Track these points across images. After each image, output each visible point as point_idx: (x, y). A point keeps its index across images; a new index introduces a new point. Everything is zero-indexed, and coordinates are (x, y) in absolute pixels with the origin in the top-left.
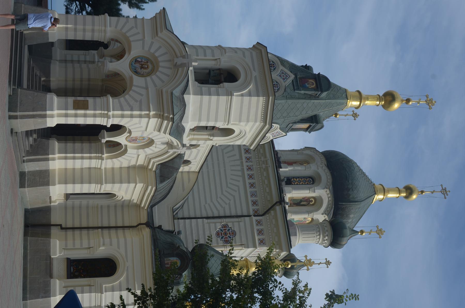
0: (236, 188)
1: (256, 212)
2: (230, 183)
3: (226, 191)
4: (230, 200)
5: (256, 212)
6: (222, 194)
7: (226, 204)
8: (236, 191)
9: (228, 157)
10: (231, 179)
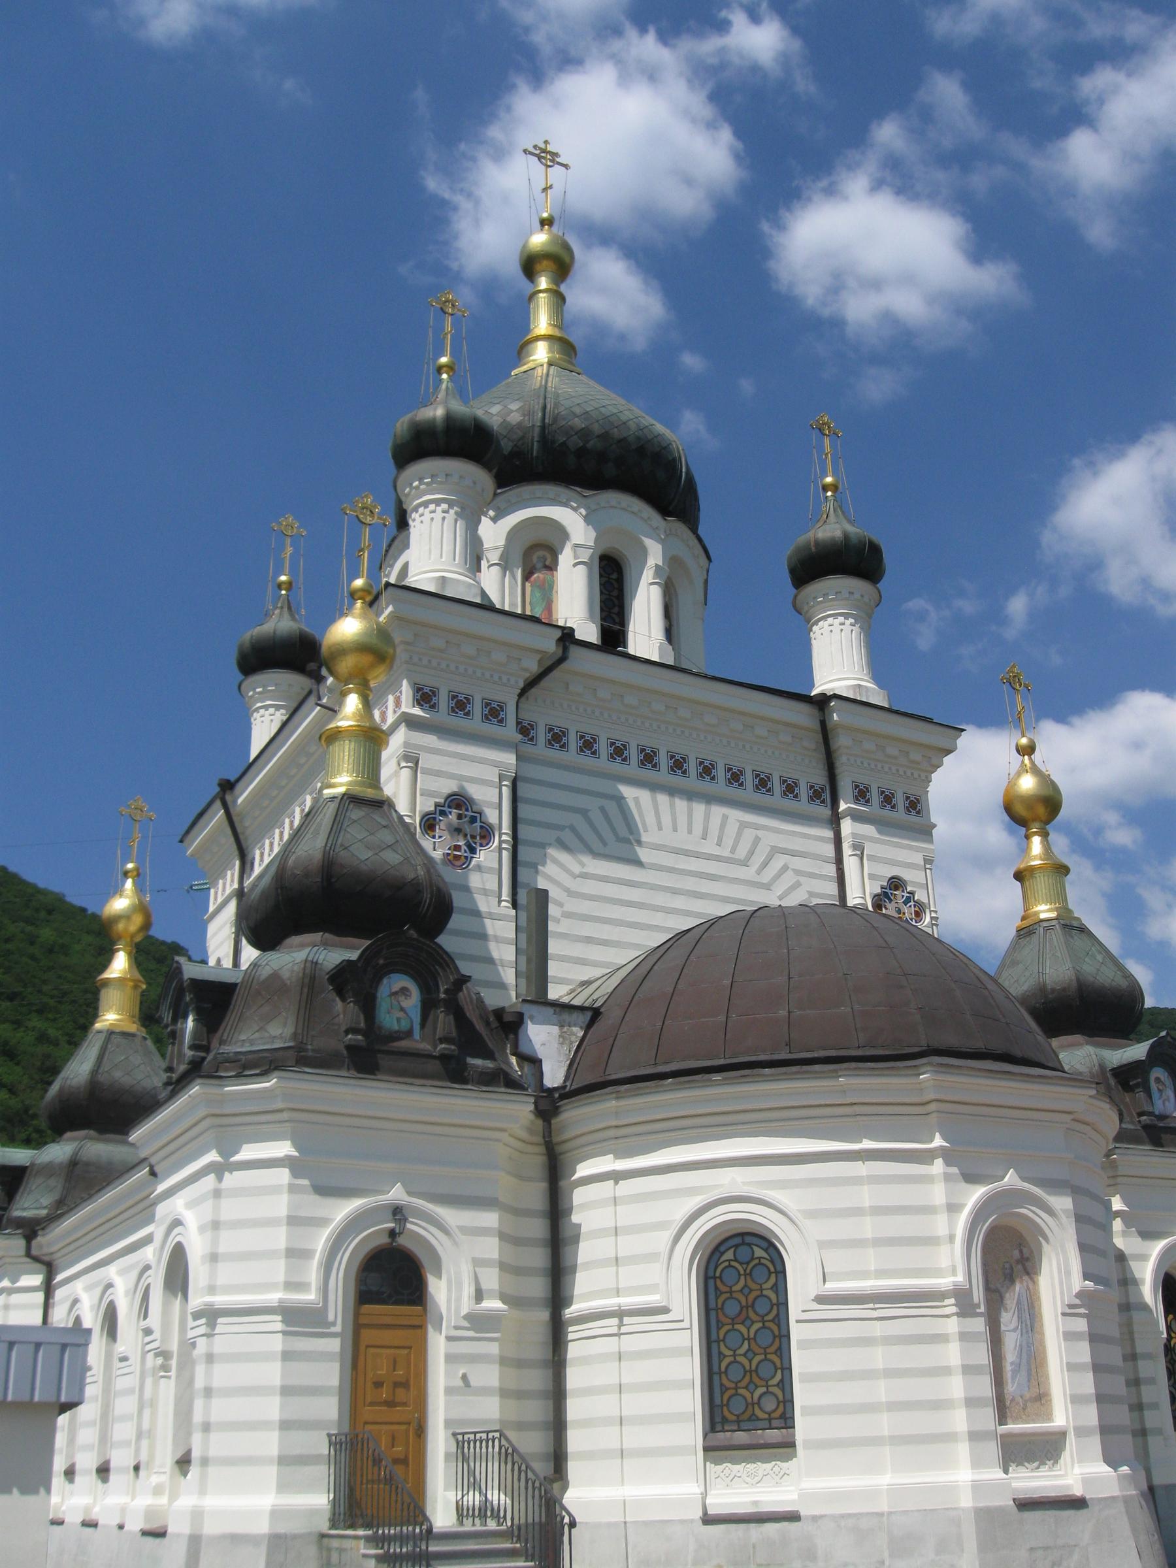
0: (749, 834)
1: (816, 795)
4: (785, 868)
5: (816, 795)
6: (767, 887)
7: (797, 885)
8: (757, 840)
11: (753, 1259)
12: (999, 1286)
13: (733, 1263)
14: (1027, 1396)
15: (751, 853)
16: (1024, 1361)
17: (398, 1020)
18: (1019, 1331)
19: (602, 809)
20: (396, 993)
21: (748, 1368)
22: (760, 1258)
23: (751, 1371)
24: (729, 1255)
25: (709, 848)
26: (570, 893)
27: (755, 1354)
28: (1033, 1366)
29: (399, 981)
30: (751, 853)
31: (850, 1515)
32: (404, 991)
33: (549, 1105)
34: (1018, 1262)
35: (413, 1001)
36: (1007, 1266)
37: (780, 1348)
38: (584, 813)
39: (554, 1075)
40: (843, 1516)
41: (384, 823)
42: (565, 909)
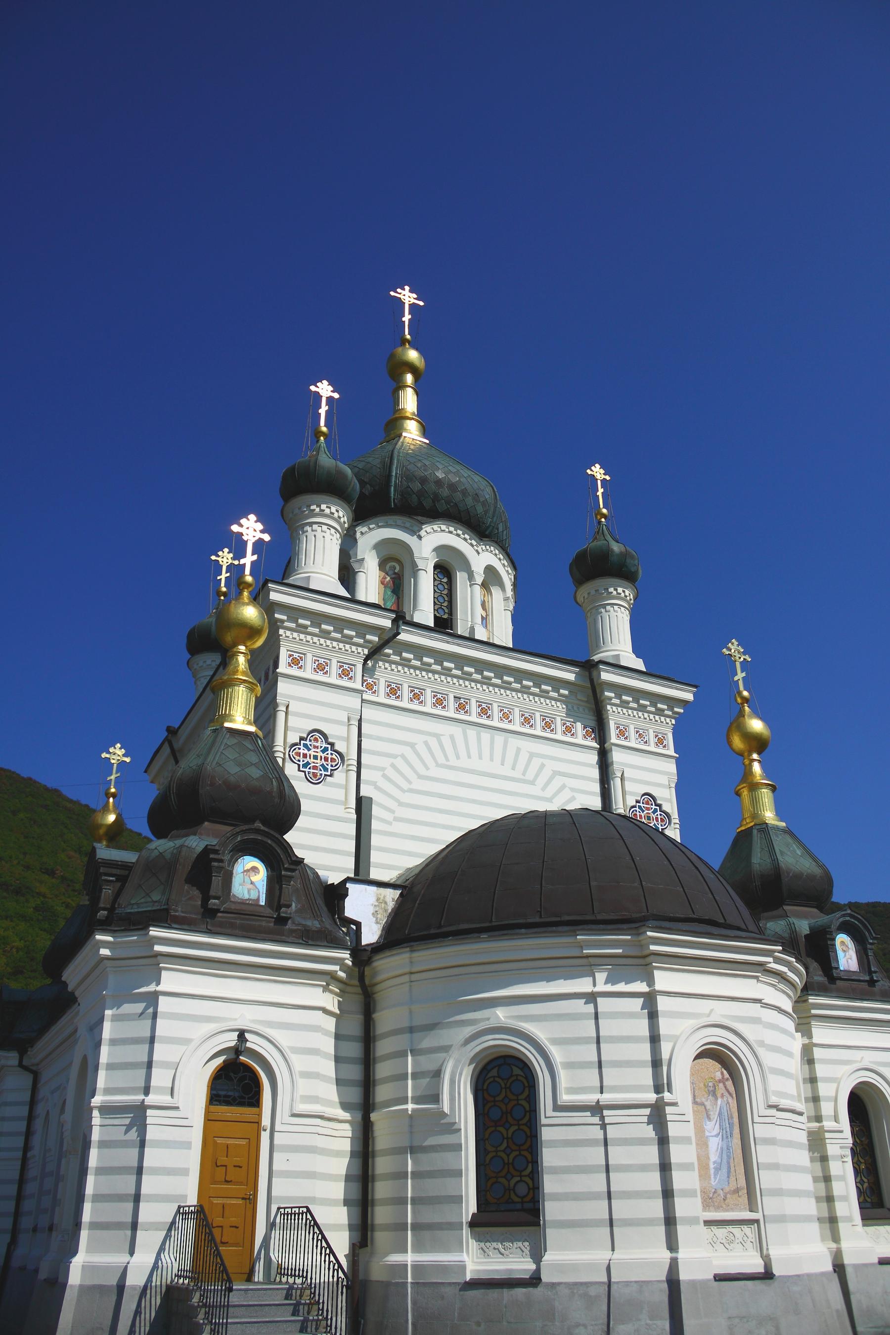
2: (524, 774)
3: (543, 789)
4: (564, 787)
8: (543, 766)
9: (458, 757)
10: (513, 769)
11: (512, 1076)
12: (704, 1100)
13: (497, 1079)
14: (727, 1189)
15: (537, 776)
16: (725, 1161)
17: (249, 891)
18: (720, 1136)
19: (426, 743)
20: (248, 871)
21: (506, 1161)
22: (517, 1075)
23: (508, 1164)
24: (494, 1072)
25: (506, 771)
26: (401, 804)
27: (512, 1151)
28: (732, 1165)
29: (250, 862)
30: (537, 776)
31: (582, 1284)
32: (254, 869)
33: (363, 957)
34: (720, 1081)
35: (261, 876)
36: (711, 1084)
37: (531, 1146)
38: (412, 746)
39: (370, 935)
40: (576, 1284)
41: (252, 748)
42: (396, 815)
